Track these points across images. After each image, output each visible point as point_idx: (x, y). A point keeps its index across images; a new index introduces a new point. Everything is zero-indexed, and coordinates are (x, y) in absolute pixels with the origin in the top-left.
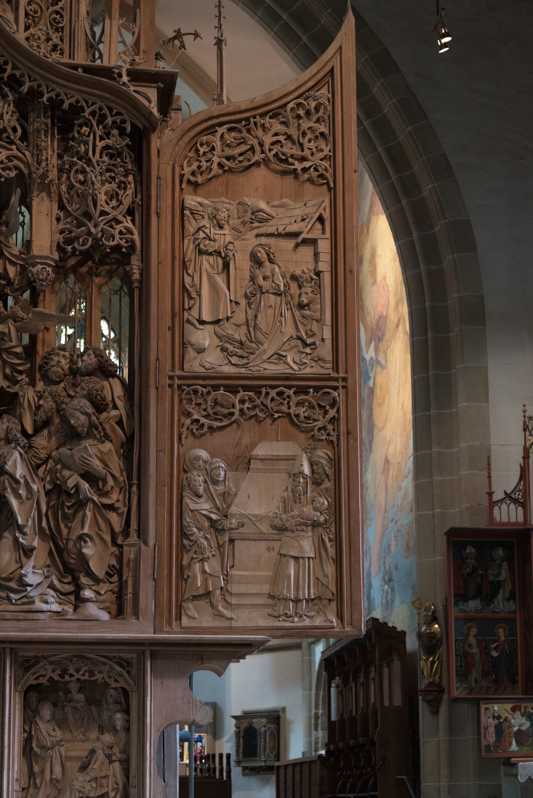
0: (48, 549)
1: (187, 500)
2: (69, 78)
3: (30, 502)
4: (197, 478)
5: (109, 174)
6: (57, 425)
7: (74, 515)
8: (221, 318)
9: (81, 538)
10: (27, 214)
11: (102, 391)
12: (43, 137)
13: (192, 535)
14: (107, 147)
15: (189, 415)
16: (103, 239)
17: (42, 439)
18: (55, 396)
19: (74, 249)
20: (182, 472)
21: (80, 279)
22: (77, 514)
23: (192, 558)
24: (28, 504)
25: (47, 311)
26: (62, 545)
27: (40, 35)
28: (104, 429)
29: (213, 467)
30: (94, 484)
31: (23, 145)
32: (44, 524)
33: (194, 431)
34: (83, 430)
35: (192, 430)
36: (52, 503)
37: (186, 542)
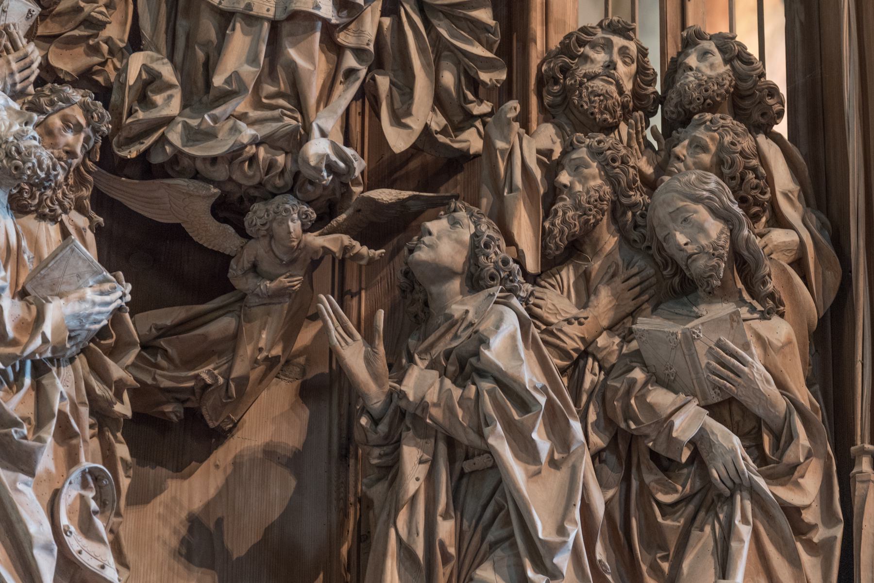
6: (610, 253)
17: (558, 295)
18: (614, 160)
24: (555, 480)
34: (715, 268)
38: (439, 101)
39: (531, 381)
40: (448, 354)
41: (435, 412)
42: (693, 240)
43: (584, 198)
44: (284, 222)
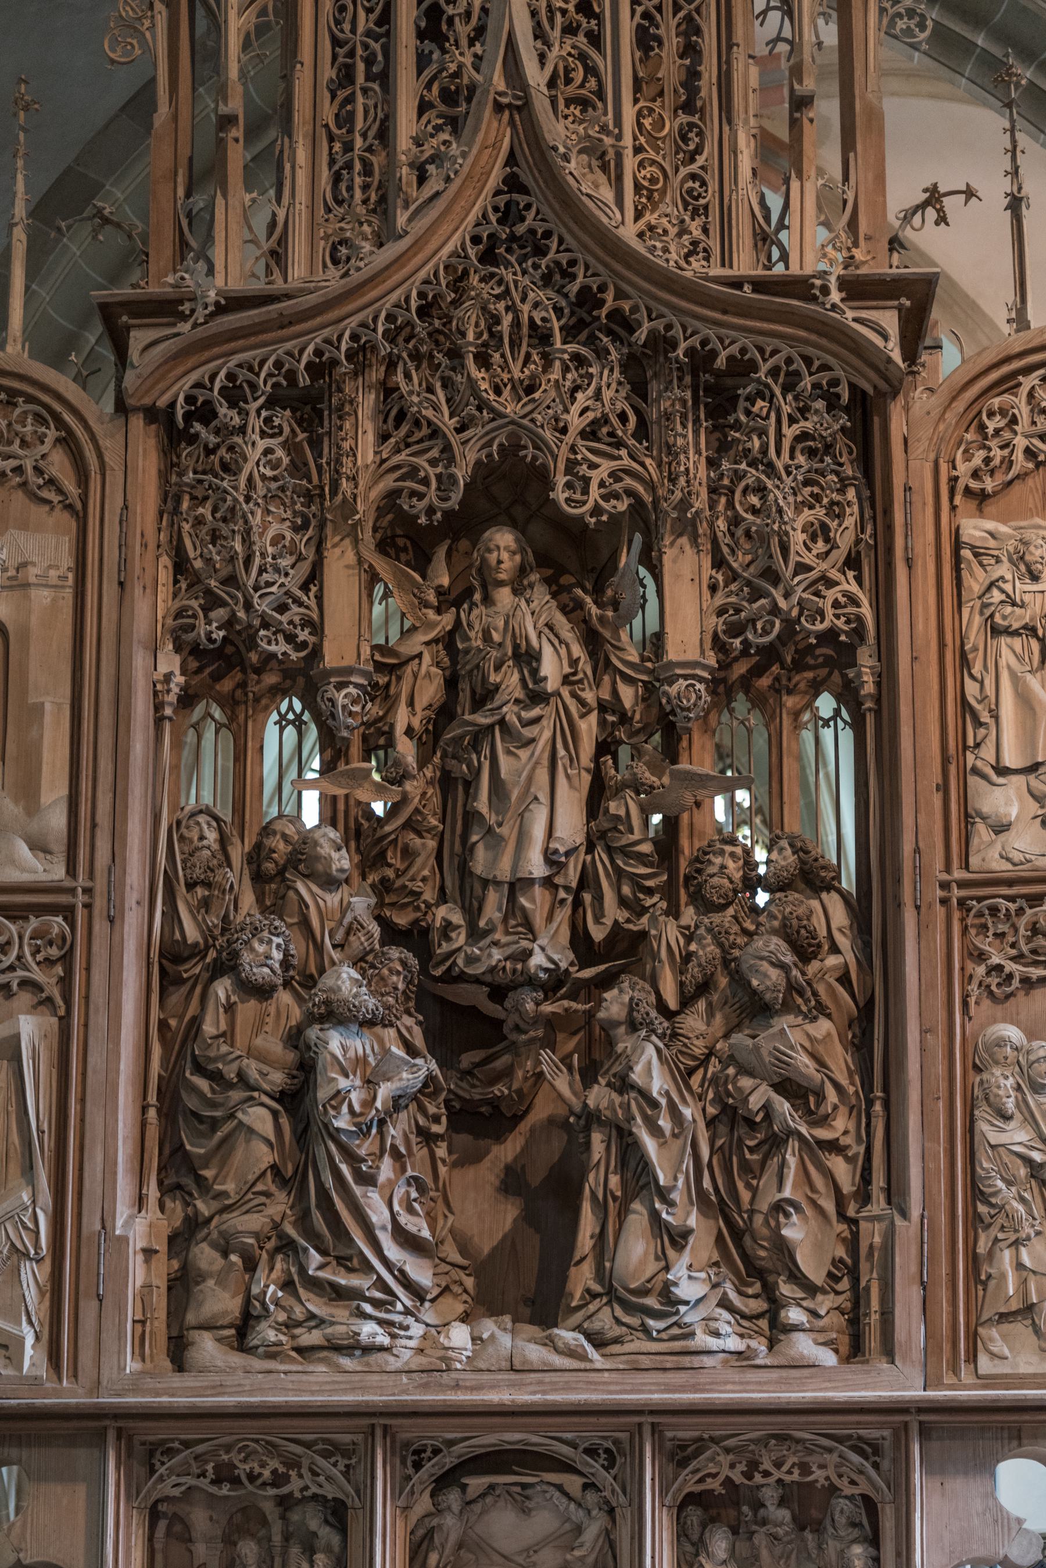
0: (715, 1232)
1: (983, 1126)
2: (725, 307)
3: (679, 1142)
4: (1002, 1081)
5: (809, 489)
7: (763, 1164)
8: (1040, 760)
9: (779, 1208)
10: (649, 581)
11: (808, 920)
12: (679, 428)
13: (995, 1194)
14: (804, 436)
15: (981, 957)
16: (803, 619)
19: (746, 643)
20: (971, 1072)
21: (758, 702)
22: (769, 1162)
23: (996, 1240)
25: (695, 768)
26: (741, 1223)
27: (669, 227)
28: (815, 994)
29: (1032, 1058)
30: (799, 1102)
31: (640, 448)
32: (707, 1183)
33: (994, 988)
34: (776, 998)
35: (988, 986)
36: (719, 1142)
37: (982, 1209)
38: (623, 902)
39: (661, 1088)
40: (614, 1076)
41: (608, 1113)
42: (762, 983)
43: (703, 960)
44: (523, 1005)
